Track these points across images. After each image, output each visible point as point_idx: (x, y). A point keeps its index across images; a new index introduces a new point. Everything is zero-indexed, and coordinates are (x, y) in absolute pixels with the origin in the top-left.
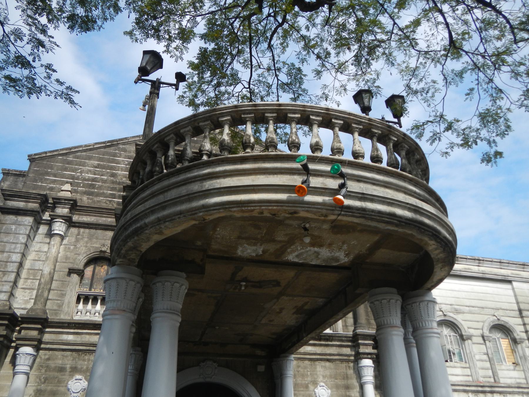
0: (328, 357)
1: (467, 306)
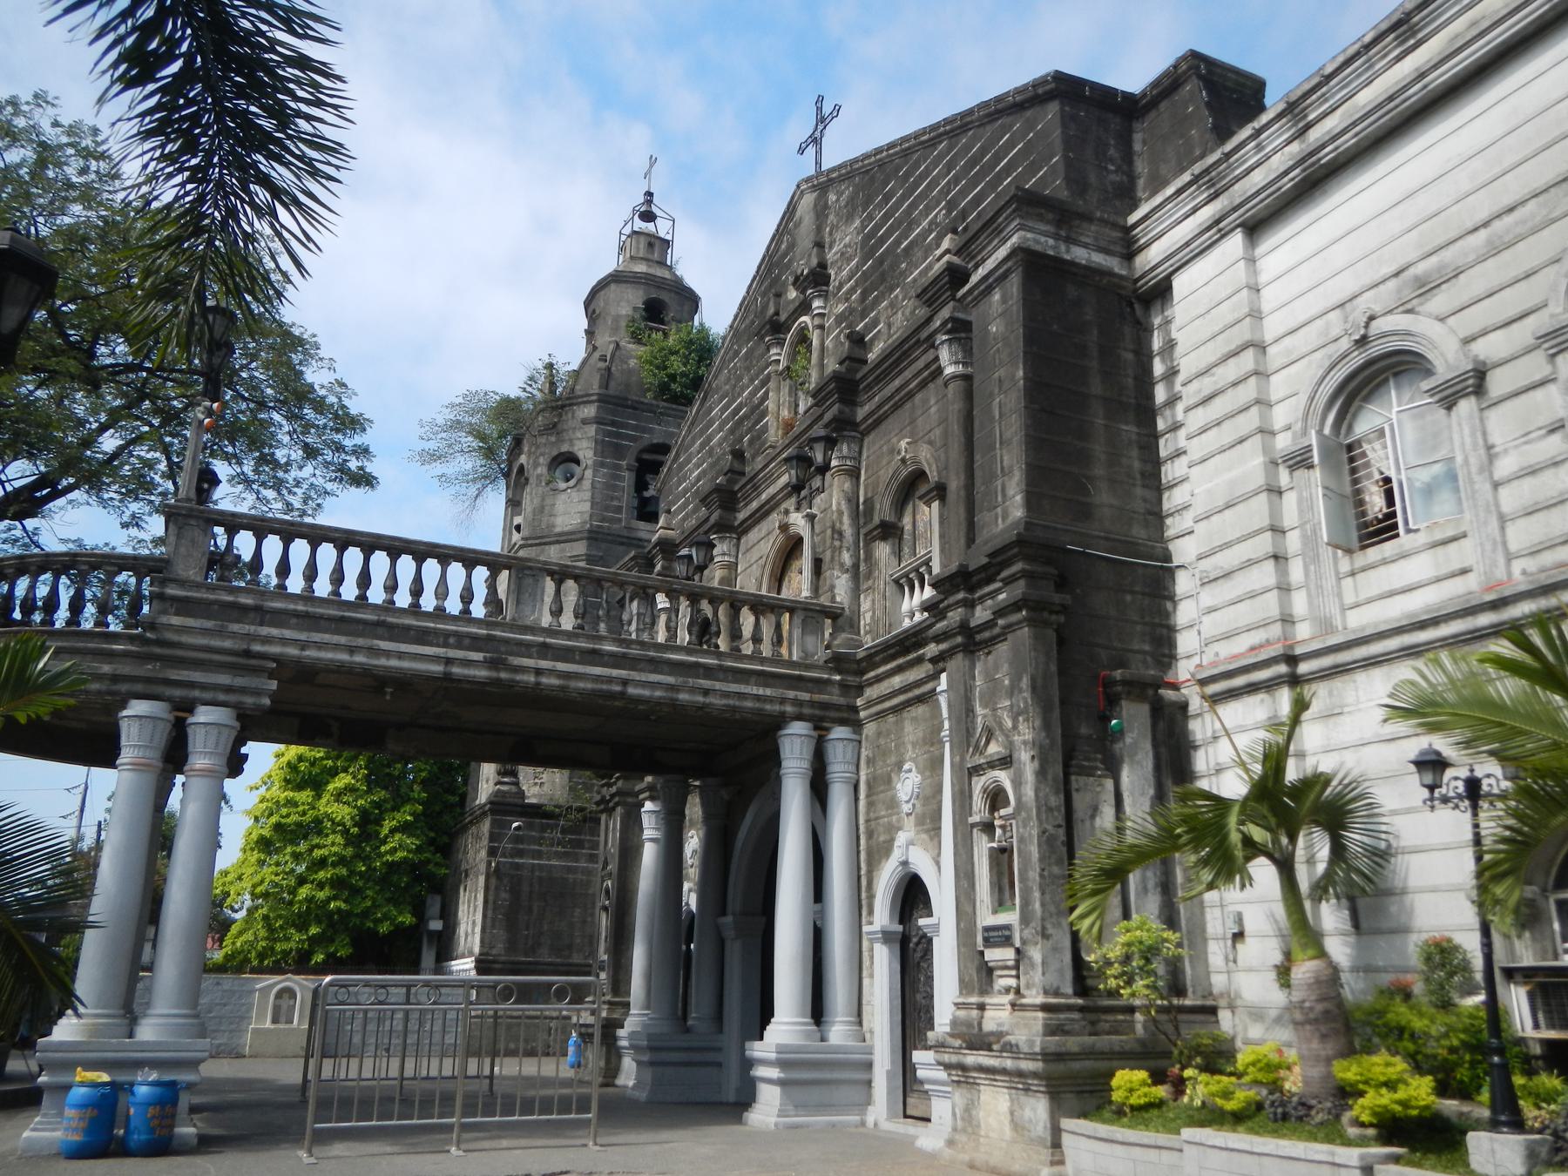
0: (917, 692)
1: (1476, 229)
